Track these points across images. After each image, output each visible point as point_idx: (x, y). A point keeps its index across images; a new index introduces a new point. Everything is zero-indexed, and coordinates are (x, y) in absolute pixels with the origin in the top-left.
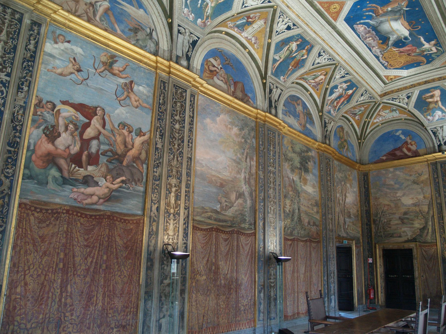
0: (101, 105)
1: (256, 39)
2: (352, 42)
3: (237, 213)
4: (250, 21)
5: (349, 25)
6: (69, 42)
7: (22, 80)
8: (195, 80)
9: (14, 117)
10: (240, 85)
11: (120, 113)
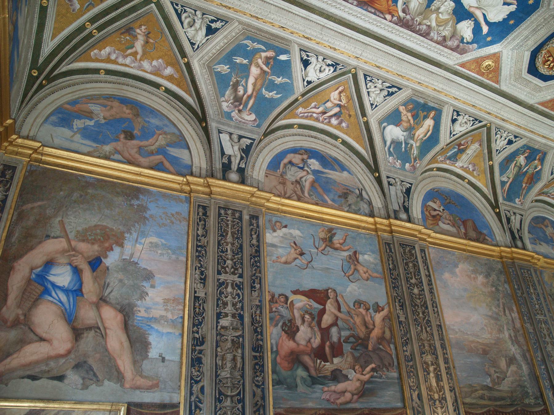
0: (331, 286)
1: (474, 165)
4: (462, 149)
6: (286, 227)
7: (253, 278)
8: (420, 232)
9: (253, 319)
10: (470, 224)
11: (352, 291)
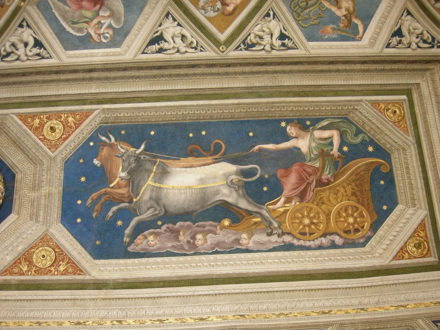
2: (179, 274)
5: (117, 257)
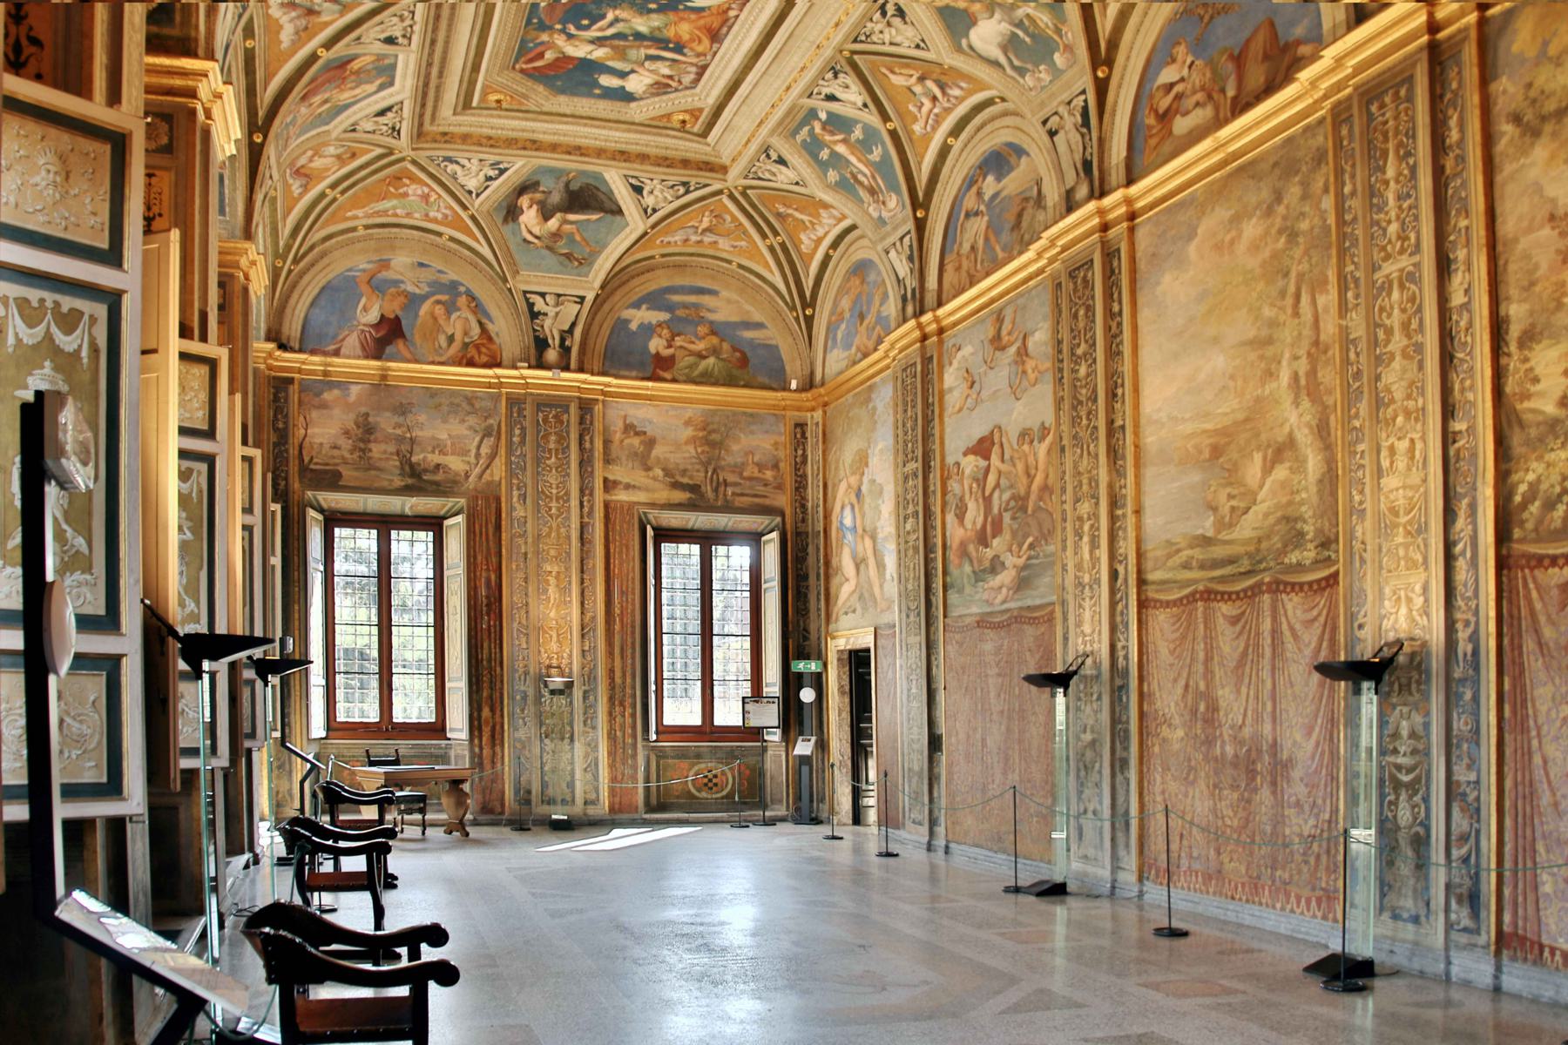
3: (1272, 519)
